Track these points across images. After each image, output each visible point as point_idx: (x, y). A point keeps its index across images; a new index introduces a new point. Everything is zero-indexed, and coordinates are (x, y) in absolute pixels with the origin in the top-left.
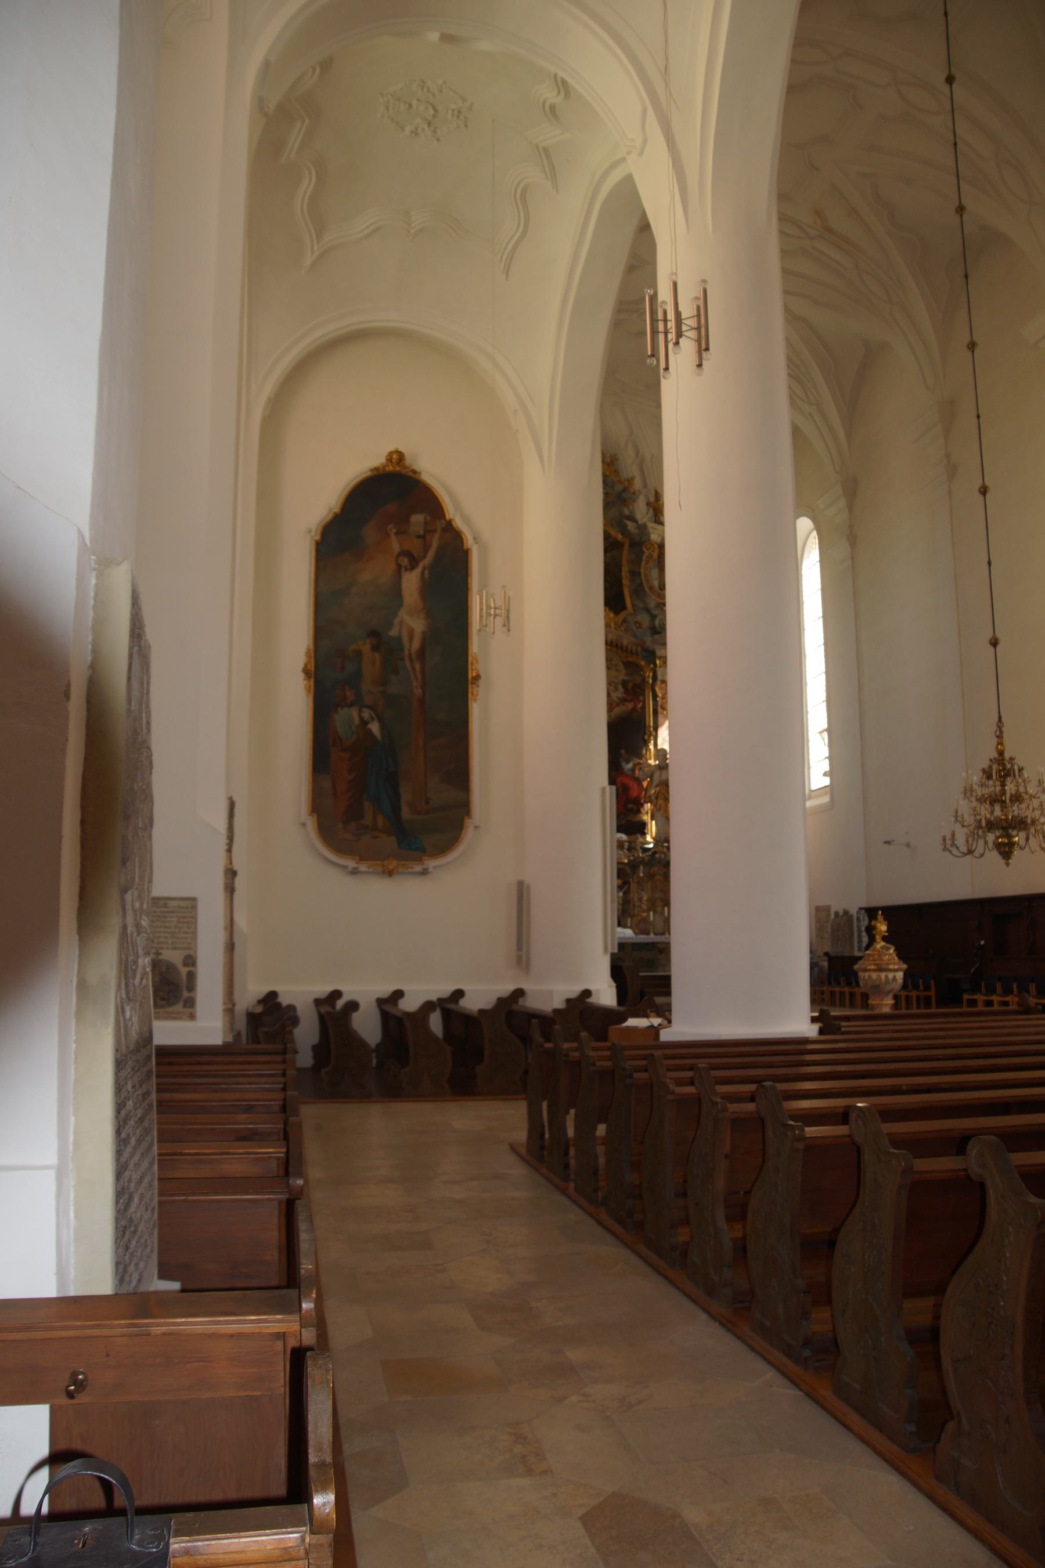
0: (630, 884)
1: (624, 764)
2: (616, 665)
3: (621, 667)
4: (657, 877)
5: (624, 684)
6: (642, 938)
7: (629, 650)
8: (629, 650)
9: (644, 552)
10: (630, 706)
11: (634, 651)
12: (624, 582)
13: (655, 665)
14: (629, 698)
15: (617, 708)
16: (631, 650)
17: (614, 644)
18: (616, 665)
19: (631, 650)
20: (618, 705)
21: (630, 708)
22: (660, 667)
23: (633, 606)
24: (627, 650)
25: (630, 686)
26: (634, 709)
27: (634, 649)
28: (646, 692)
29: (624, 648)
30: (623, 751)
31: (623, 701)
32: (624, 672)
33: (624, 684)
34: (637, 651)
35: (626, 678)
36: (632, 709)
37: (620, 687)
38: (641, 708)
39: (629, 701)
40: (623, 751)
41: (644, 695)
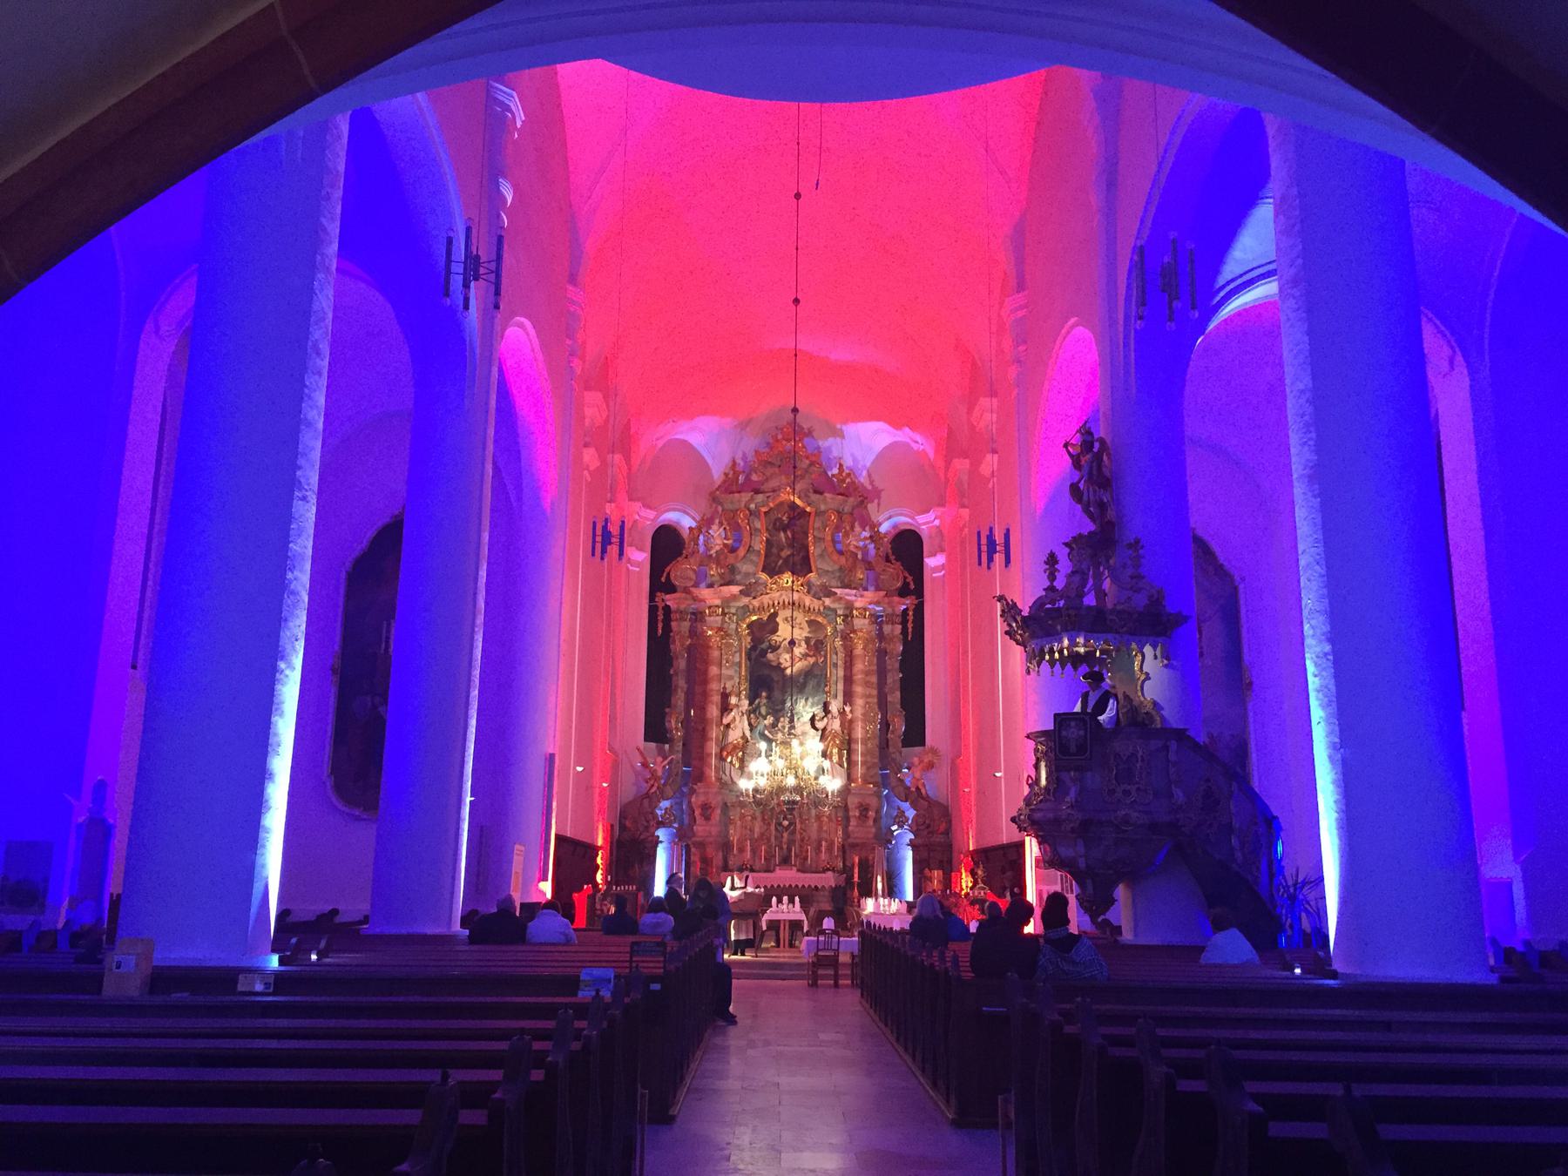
2: (800, 624)
3: (805, 625)
5: (807, 640)
10: (812, 660)
14: (811, 653)
18: (800, 624)
26: (815, 664)
31: (805, 656)
32: (808, 630)
34: (819, 610)
35: (808, 635)
39: (811, 656)
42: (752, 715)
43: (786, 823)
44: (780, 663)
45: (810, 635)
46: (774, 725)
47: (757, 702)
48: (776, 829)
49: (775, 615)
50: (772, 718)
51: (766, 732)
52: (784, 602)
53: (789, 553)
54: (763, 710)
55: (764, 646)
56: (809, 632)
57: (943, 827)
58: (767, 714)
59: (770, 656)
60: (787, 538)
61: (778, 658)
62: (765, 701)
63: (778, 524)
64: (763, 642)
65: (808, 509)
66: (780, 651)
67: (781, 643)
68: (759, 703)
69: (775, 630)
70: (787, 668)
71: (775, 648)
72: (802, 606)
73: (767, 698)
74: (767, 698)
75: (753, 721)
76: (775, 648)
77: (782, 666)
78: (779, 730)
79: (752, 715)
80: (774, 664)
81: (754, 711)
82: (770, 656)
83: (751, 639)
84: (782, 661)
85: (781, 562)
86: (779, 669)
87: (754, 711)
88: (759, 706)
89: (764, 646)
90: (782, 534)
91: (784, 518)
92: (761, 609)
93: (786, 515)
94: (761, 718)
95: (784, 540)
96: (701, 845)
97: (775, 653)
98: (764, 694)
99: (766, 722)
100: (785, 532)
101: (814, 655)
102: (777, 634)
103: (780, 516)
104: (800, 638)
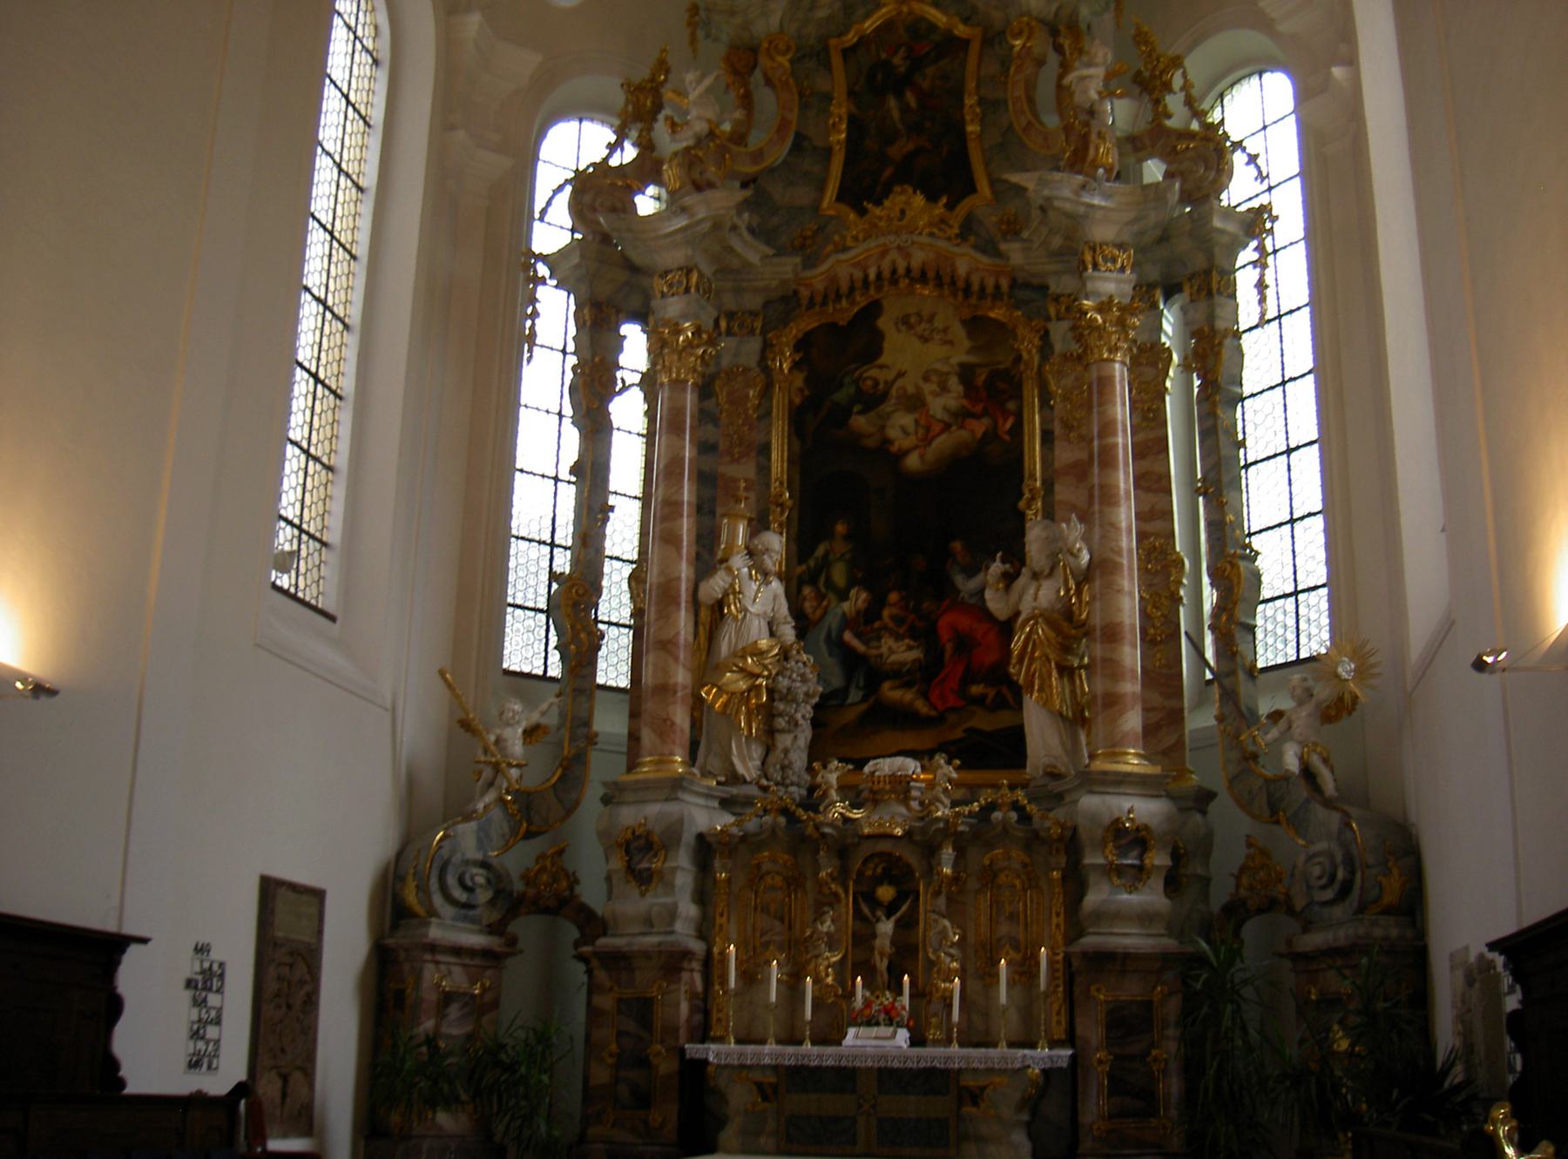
0: (917, 898)
1: (959, 579)
2: (945, 330)
3: (959, 332)
4: (1002, 878)
5: (966, 373)
6: (933, 1055)
7: (976, 287)
8: (976, 287)
9: (1013, 47)
10: (979, 427)
11: (990, 289)
12: (970, 128)
13: (1048, 319)
14: (978, 408)
15: (944, 437)
16: (983, 288)
17: (931, 275)
18: (945, 330)
19: (983, 288)
20: (947, 427)
21: (979, 435)
22: (1059, 319)
23: (993, 182)
24: (967, 290)
25: (981, 379)
26: (991, 436)
27: (990, 283)
28: (1026, 393)
29: (961, 284)
30: (957, 546)
31: (961, 416)
32: (967, 344)
33: (966, 373)
34: (997, 287)
35: (965, 358)
36: (985, 434)
37: (954, 383)
38: (1009, 432)
39: (977, 417)
40: (957, 546)
41: (1018, 396)
42: (807, 591)
43: (886, 893)
44: (887, 441)
45: (972, 359)
46: (870, 614)
47: (821, 550)
48: (858, 914)
49: (874, 309)
50: (864, 596)
52: (894, 272)
53: (911, 146)
54: (839, 575)
55: (841, 396)
56: (969, 352)
57: (1393, 888)
58: (852, 582)
59: (860, 422)
60: (905, 109)
61: (883, 427)
62: (840, 547)
63: (880, 77)
64: (841, 385)
65: (961, 30)
66: (887, 407)
67: (889, 385)
68: (827, 553)
69: (872, 348)
70: (906, 453)
71: (872, 400)
72: (946, 279)
73: (847, 537)
74: (847, 537)
75: (808, 606)
76: (872, 400)
77: (894, 448)
78: (885, 628)
79: (807, 591)
80: (871, 443)
81: (812, 579)
82: (860, 422)
83: (807, 380)
84: (893, 433)
85: (888, 172)
86: (885, 455)
87: (812, 579)
88: (825, 564)
89: (841, 396)
90: (892, 103)
91: (897, 60)
92: (833, 293)
93: (902, 52)
94: (831, 595)
95: (896, 114)
96: (619, 961)
97: (872, 414)
98: (840, 528)
99: (846, 606)
100: (899, 95)
101: (985, 413)
102: (882, 361)
103: (884, 56)
104: (945, 369)
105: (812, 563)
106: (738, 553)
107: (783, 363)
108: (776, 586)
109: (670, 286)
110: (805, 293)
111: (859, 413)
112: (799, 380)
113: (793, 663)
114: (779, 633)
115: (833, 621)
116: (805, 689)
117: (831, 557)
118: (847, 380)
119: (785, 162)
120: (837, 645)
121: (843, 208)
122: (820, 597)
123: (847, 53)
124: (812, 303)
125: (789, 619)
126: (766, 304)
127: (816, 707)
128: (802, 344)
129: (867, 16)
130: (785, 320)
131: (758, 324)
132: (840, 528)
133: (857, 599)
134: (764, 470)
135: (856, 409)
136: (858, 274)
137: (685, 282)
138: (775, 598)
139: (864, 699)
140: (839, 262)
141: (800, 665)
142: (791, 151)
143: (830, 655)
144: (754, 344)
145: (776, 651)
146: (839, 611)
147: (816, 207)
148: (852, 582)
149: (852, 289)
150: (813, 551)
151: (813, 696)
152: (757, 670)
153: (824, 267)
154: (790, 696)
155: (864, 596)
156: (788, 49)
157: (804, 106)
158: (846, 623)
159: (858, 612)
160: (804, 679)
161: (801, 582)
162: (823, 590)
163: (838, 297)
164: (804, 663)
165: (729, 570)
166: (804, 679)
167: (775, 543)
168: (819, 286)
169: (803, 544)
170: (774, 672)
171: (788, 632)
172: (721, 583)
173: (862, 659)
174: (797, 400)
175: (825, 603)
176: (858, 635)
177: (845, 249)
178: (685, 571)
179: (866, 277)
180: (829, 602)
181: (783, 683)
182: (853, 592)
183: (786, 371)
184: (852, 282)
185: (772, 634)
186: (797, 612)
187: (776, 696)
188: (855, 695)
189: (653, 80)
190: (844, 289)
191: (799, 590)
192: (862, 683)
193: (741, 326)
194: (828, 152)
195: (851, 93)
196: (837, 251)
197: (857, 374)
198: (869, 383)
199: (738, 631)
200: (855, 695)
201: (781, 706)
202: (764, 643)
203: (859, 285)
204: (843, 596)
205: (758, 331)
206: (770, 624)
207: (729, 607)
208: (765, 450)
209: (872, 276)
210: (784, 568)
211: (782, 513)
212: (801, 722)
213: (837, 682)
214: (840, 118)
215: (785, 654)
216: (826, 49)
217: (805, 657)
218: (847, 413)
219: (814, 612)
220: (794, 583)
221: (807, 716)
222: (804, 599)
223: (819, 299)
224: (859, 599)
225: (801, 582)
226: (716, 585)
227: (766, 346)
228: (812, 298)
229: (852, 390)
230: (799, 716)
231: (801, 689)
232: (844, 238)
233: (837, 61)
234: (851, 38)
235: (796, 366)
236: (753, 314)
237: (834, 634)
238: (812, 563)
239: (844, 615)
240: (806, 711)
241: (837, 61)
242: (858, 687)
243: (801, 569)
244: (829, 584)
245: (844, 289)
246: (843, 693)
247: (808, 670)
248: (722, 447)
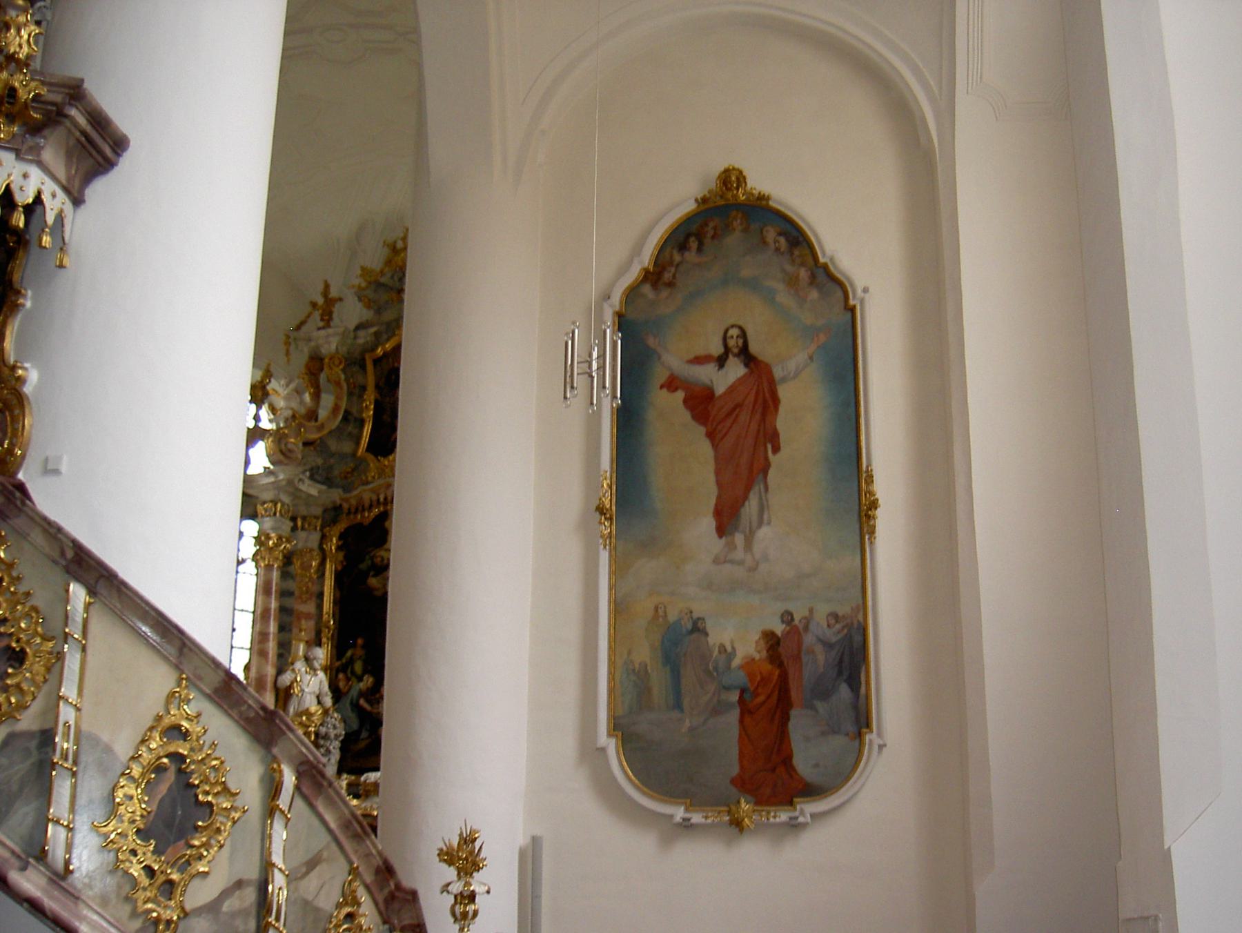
42: (341, 676)
47: (349, 654)
50: (371, 680)
51: (362, 702)
54: (358, 667)
55: (363, 566)
62: (360, 652)
73: (363, 647)
74: (363, 647)
75: (342, 684)
79: (341, 676)
81: (343, 669)
87: (343, 669)
88: (351, 661)
92: (359, 508)
94: (354, 679)
98: (360, 641)
99: (362, 685)
105: (344, 661)
106: (299, 660)
107: (333, 544)
108: (321, 675)
109: (266, 510)
110: (346, 506)
111: (373, 576)
112: (341, 556)
113: (329, 719)
114: (322, 702)
115: (354, 693)
116: (335, 732)
117: (354, 657)
118: (367, 557)
119: (338, 428)
120: (356, 706)
121: (370, 457)
122: (348, 679)
123: (377, 361)
124: (349, 513)
125: (329, 693)
126: (325, 511)
127: (342, 742)
128: (341, 537)
129: (388, 340)
130: (334, 522)
131: (319, 523)
132: (360, 641)
133: (367, 681)
134: (320, 606)
135: (372, 573)
136: (374, 497)
137: (273, 509)
138: (321, 682)
139: (369, 736)
140: (365, 491)
141: (333, 720)
142: (341, 421)
143: (352, 710)
144: (315, 537)
145: (320, 712)
146: (358, 688)
147: (354, 454)
148: (365, 671)
149: (371, 506)
150: (345, 653)
151: (340, 735)
152: (308, 723)
153: (355, 493)
154: (326, 737)
155: (371, 680)
156: (340, 363)
157: (350, 394)
158: (361, 694)
159: (368, 689)
160: (335, 727)
161: (338, 671)
162: (349, 675)
163: (363, 510)
164: (336, 719)
165: (293, 670)
166: (335, 727)
167: (321, 654)
168: (354, 502)
169: (339, 650)
170: (318, 724)
171: (328, 701)
172: (289, 677)
173: (370, 713)
174: (339, 568)
175: (350, 683)
176: (368, 701)
177: (367, 483)
178: (270, 671)
179: (378, 500)
180: (353, 683)
181: (323, 730)
182: (365, 677)
183: (334, 551)
184: (371, 501)
185: (319, 702)
186: (334, 687)
187: (320, 736)
188: (364, 734)
189: (262, 382)
190: (367, 504)
191: (337, 676)
192: (368, 728)
193: (309, 525)
194: (362, 423)
195: (377, 387)
196: (363, 484)
197: (372, 554)
198: (379, 559)
199: (299, 704)
200: (364, 734)
201: (322, 742)
202: (314, 708)
203: (375, 503)
204: (360, 679)
205: (318, 528)
206: (318, 697)
207: (294, 690)
208: (321, 595)
209: (382, 499)
210: (329, 663)
211: (329, 632)
212: (333, 750)
213: (355, 725)
214: (370, 403)
215: (326, 712)
216: (364, 359)
217: (336, 715)
218: (365, 575)
219: (345, 687)
220: (334, 672)
221: (336, 747)
222: (339, 680)
223: (353, 510)
224: (368, 681)
225: (338, 671)
226: (286, 678)
227: (323, 537)
228: (349, 509)
229: (369, 562)
230: (331, 747)
231: (332, 733)
232: (367, 478)
233: (370, 367)
234: (379, 351)
235: (339, 548)
236: (316, 518)
237: (354, 701)
238: (344, 661)
239: (360, 689)
240: (337, 744)
241: (370, 367)
242: (366, 729)
243: (338, 664)
244: (353, 673)
245: (367, 504)
246: (358, 733)
247: (337, 723)
248: (297, 593)
